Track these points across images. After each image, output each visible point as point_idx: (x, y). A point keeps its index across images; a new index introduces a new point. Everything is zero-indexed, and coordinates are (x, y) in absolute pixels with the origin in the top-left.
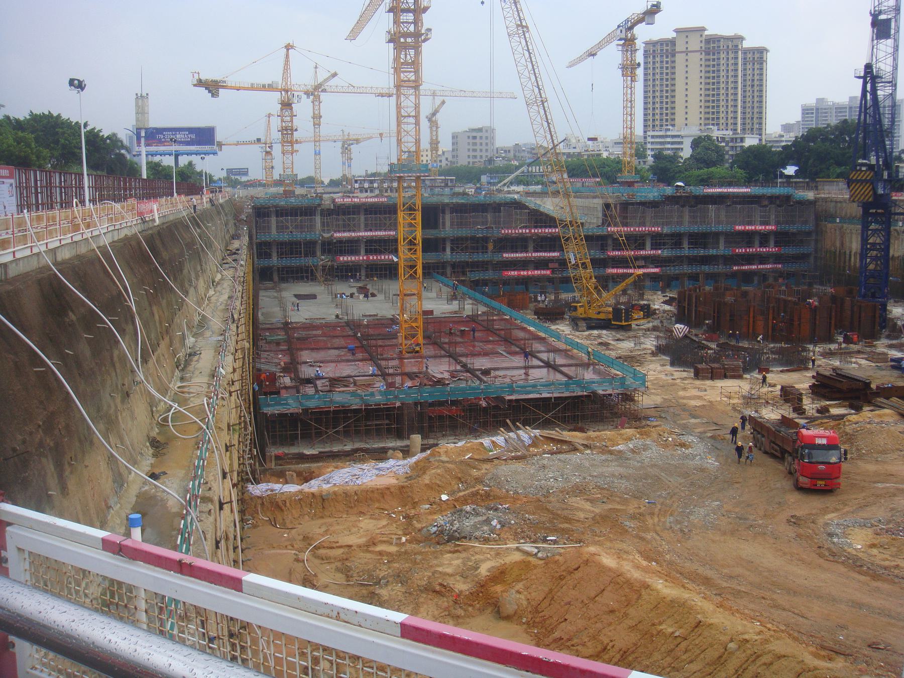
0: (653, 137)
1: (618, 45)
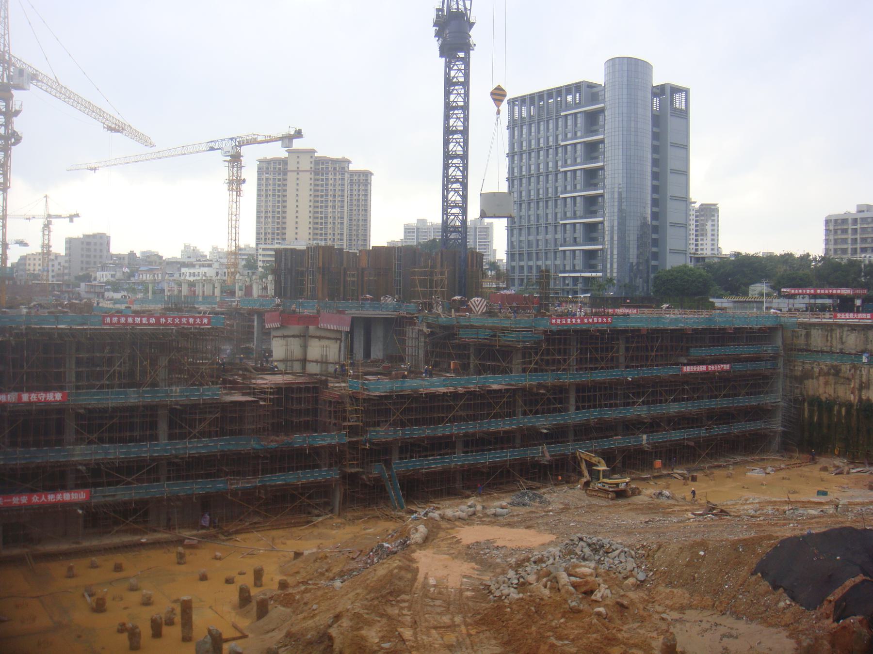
0: (264, 249)
1: (225, 161)
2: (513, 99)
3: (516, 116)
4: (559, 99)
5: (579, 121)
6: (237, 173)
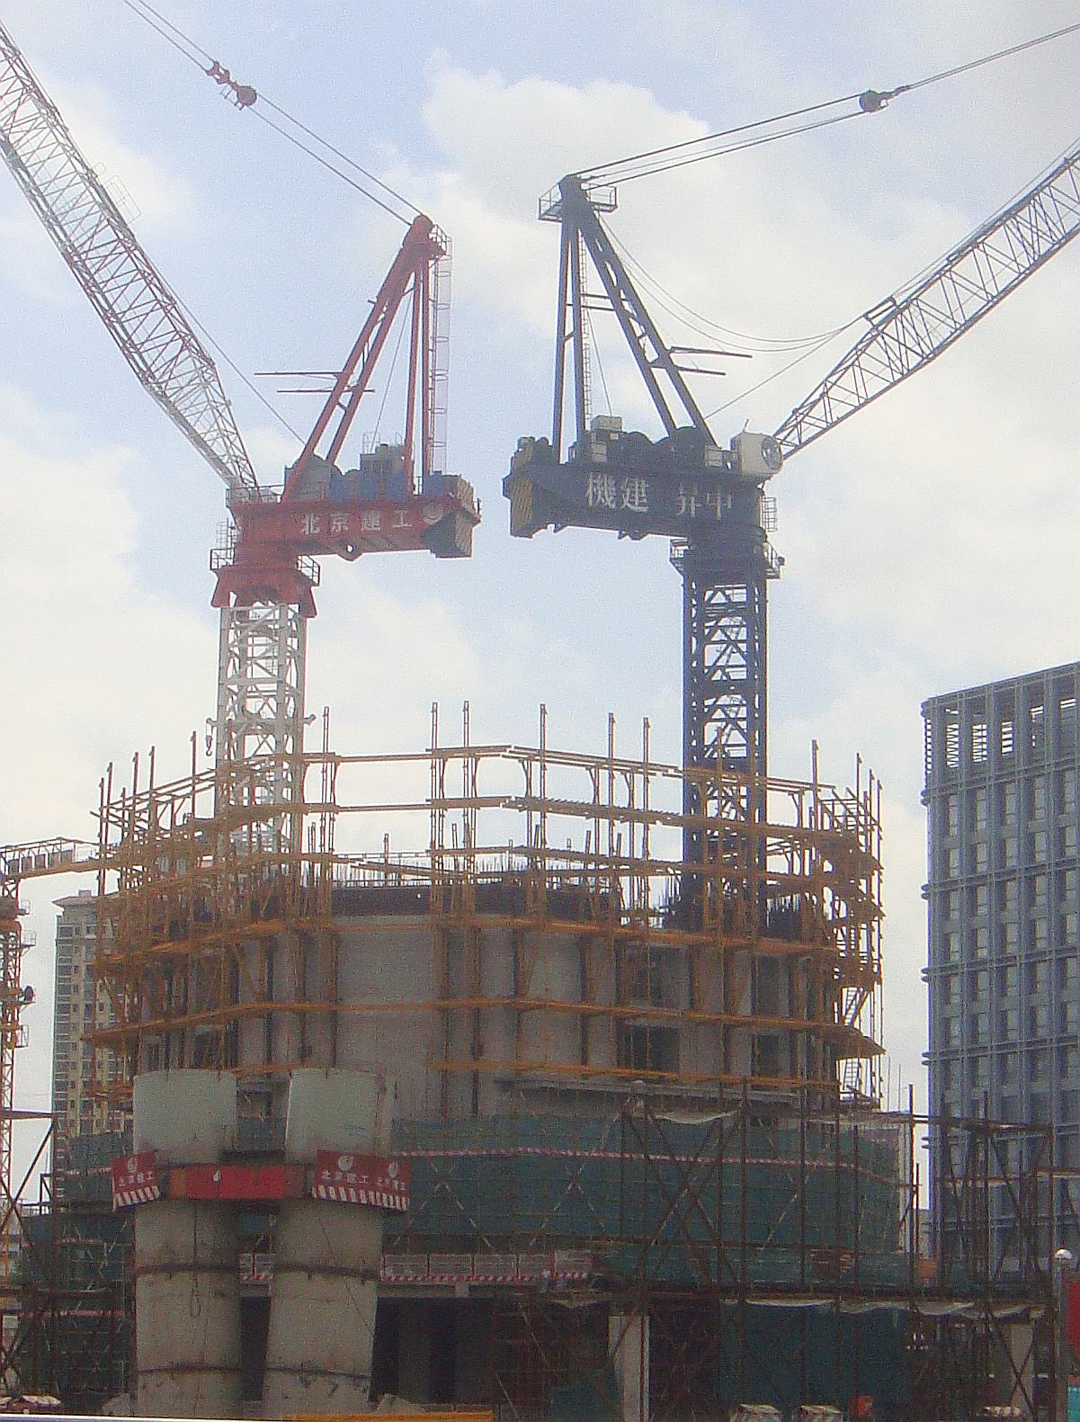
3: (953, 761)
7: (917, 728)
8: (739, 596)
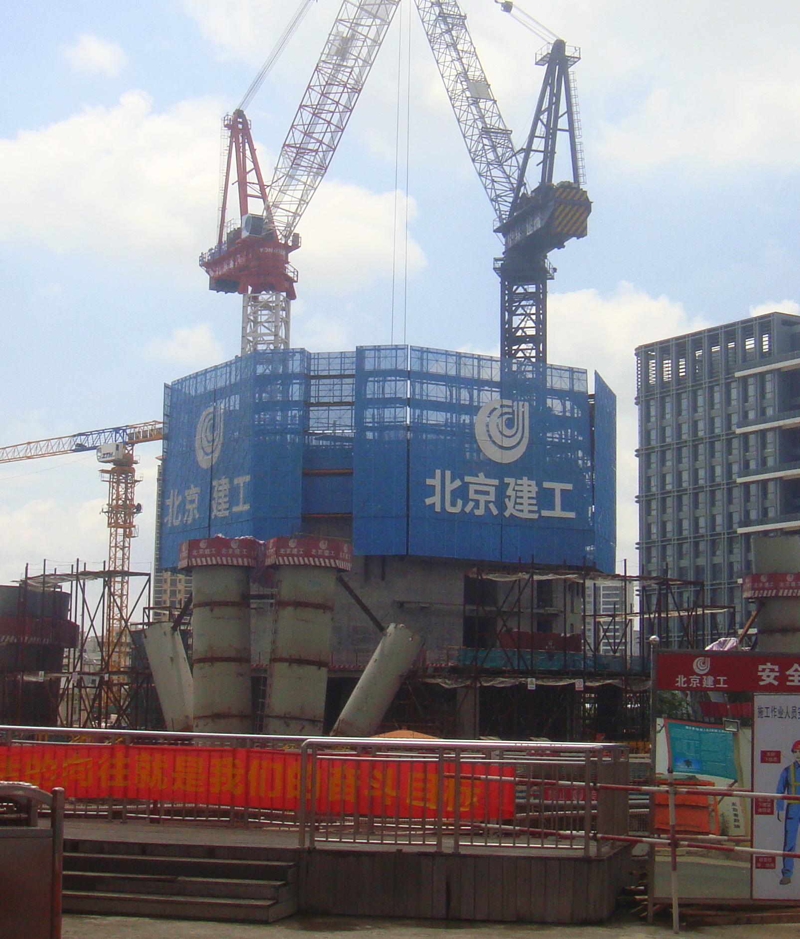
1: (103, 471)
2: (646, 346)
3: (652, 380)
4: (731, 345)
5: (769, 387)
6: (126, 493)
7: (632, 363)
8: (532, 288)
